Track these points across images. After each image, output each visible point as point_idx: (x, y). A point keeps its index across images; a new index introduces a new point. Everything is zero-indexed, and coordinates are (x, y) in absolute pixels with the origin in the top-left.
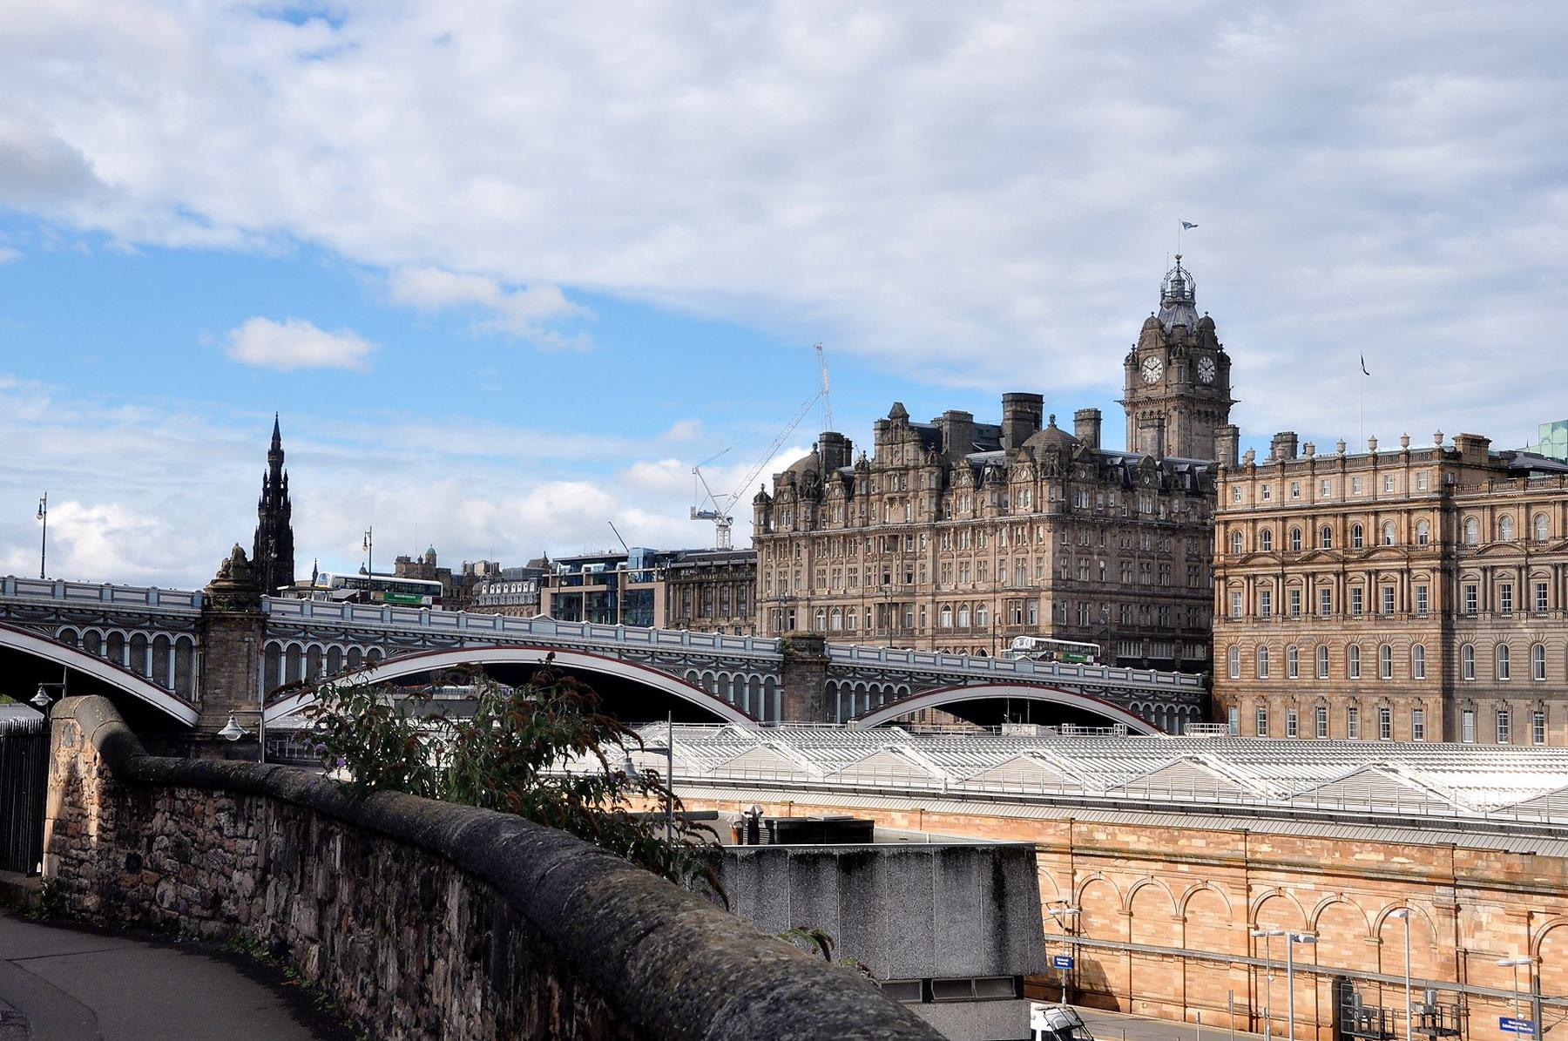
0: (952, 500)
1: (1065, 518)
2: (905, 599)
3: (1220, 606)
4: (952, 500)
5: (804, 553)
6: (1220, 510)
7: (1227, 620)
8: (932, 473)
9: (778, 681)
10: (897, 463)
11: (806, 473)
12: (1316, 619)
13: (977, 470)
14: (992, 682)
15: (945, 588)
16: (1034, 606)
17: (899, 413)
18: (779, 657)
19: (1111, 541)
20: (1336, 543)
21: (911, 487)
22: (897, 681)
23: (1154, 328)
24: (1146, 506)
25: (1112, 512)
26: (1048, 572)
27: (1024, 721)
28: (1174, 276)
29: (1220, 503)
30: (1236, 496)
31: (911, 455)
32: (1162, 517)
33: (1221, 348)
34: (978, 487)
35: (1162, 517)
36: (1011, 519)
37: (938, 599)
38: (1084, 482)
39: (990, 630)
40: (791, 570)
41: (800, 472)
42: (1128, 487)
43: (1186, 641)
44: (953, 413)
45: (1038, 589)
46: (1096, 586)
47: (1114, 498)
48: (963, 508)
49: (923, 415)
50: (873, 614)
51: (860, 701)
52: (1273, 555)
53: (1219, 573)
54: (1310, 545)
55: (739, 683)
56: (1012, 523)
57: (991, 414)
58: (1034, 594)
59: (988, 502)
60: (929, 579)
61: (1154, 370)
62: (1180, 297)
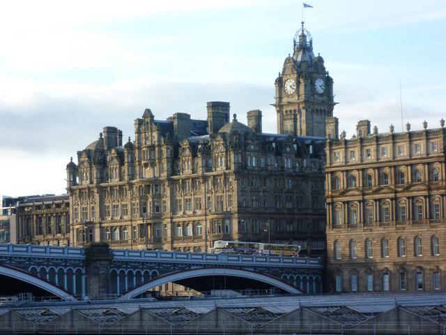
1: (242, 171)
2: (155, 221)
5: (97, 197)
6: (328, 165)
8: (167, 149)
9: (83, 272)
11: (96, 150)
13: (193, 147)
14: (205, 266)
17: (148, 113)
18: (83, 257)
22: (151, 268)
23: (288, 60)
24: (288, 164)
25: (270, 168)
26: (235, 204)
27: (223, 289)
28: (300, 33)
29: (328, 162)
30: (338, 158)
31: (156, 139)
32: (297, 170)
33: (327, 73)
34: (194, 156)
35: (297, 170)
36: (214, 173)
37: (174, 220)
38: (254, 151)
41: (93, 148)
43: (313, 239)
46: (262, 210)
47: (272, 161)
49: (162, 116)
50: (137, 230)
51: (130, 281)
53: (329, 200)
54: (377, 183)
55: (61, 273)
56: (214, 176)
59: (200, 164)
61: (290, 85)
62: (304, 46)
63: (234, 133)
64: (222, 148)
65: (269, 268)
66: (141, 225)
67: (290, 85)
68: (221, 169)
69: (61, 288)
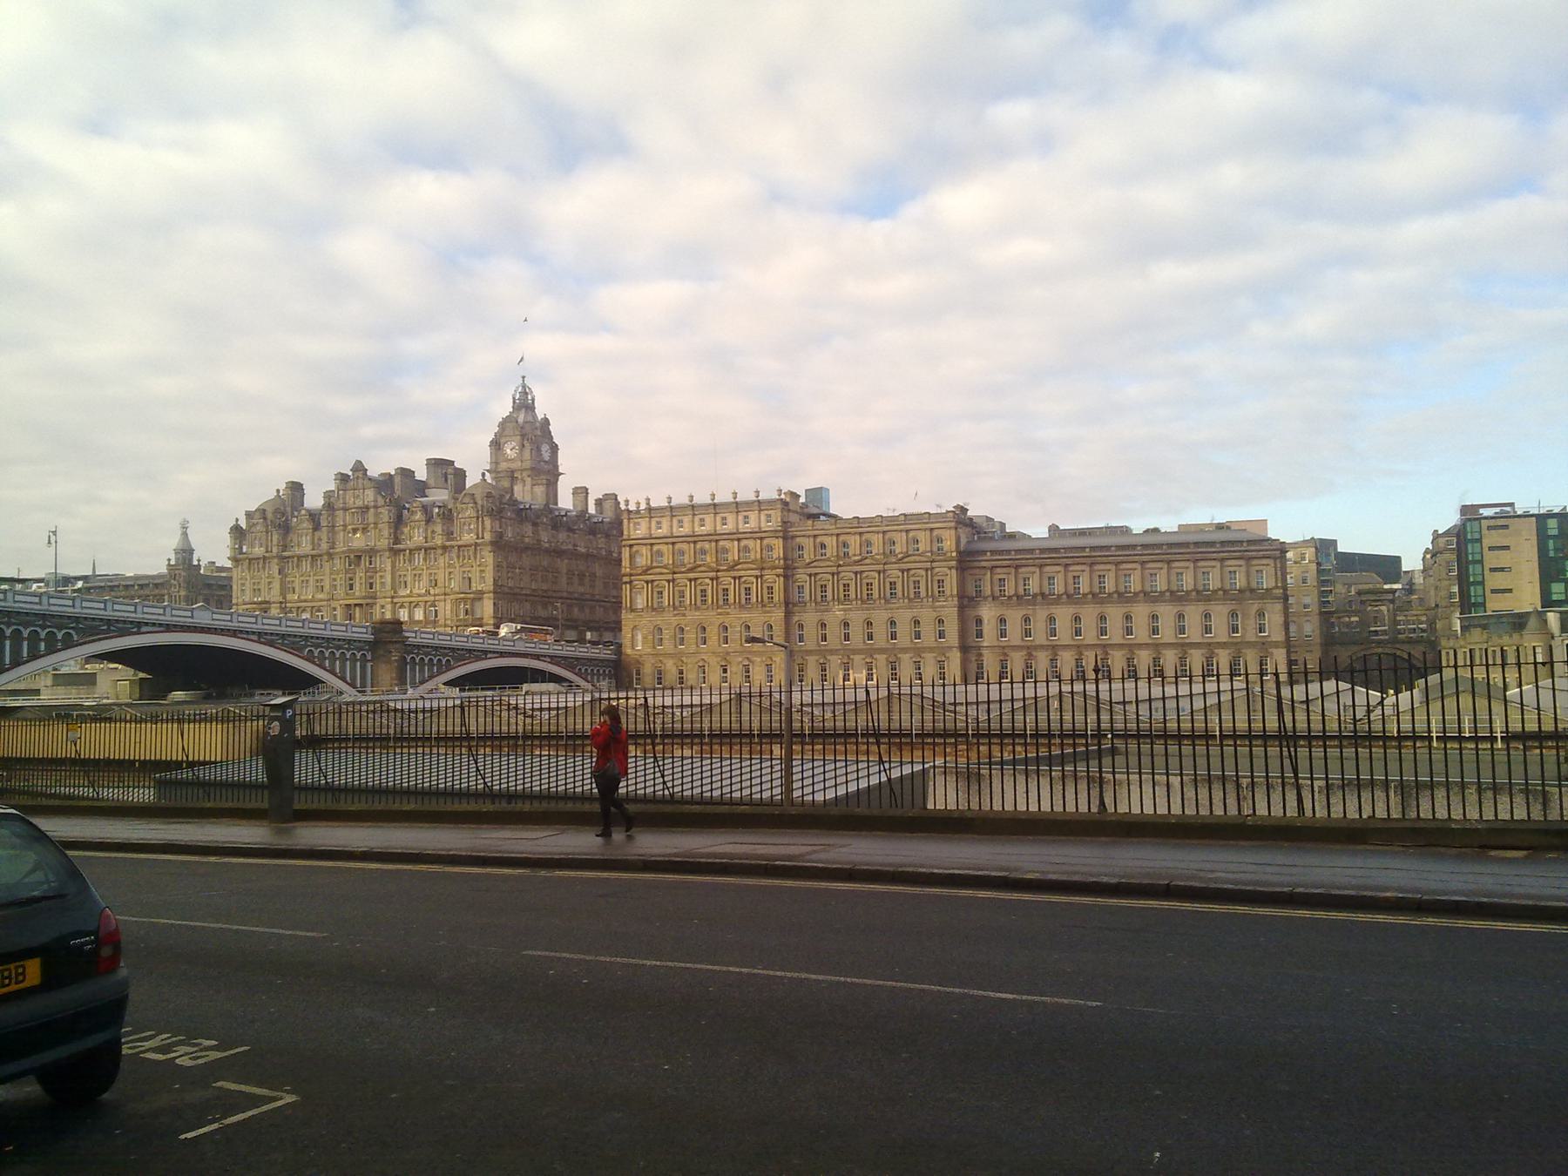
0: (406, 530)
1: (498, 544)
3: (626, 601)
4: (406, 530)
7: (632, 610)
10: (359, 503)
11: (276, 511)
12: (697, 609)
13: (426, 509)
14: (502, 654)
15: (402, 592)
16: (477, 604)
17: (359, 468)
19: (527, 561)
20: (709, 559)
21: (371, 519)
26: (490, 581)
31: (371, 498)
34: (429, 520)
39: (442, 622)
40: (264, 581)
41: (270, 510)
42: (535, 524)
44: (403, 469)
45: (482, 592)
47: (528, 529)
48: (415, 536)
52: (665, 567)
53: (626, 579)
55: (343, 658)
57: (421, 474)
58: (479, 596)
60: (388, 587)
61: (510, 450)
62: (524, 403)
63: (489, 496)
64: (470, 512)
65: (565, 658)
66: (348, 606)
67: (510, 450)
68: (468, 538)
69: (343, 679)
